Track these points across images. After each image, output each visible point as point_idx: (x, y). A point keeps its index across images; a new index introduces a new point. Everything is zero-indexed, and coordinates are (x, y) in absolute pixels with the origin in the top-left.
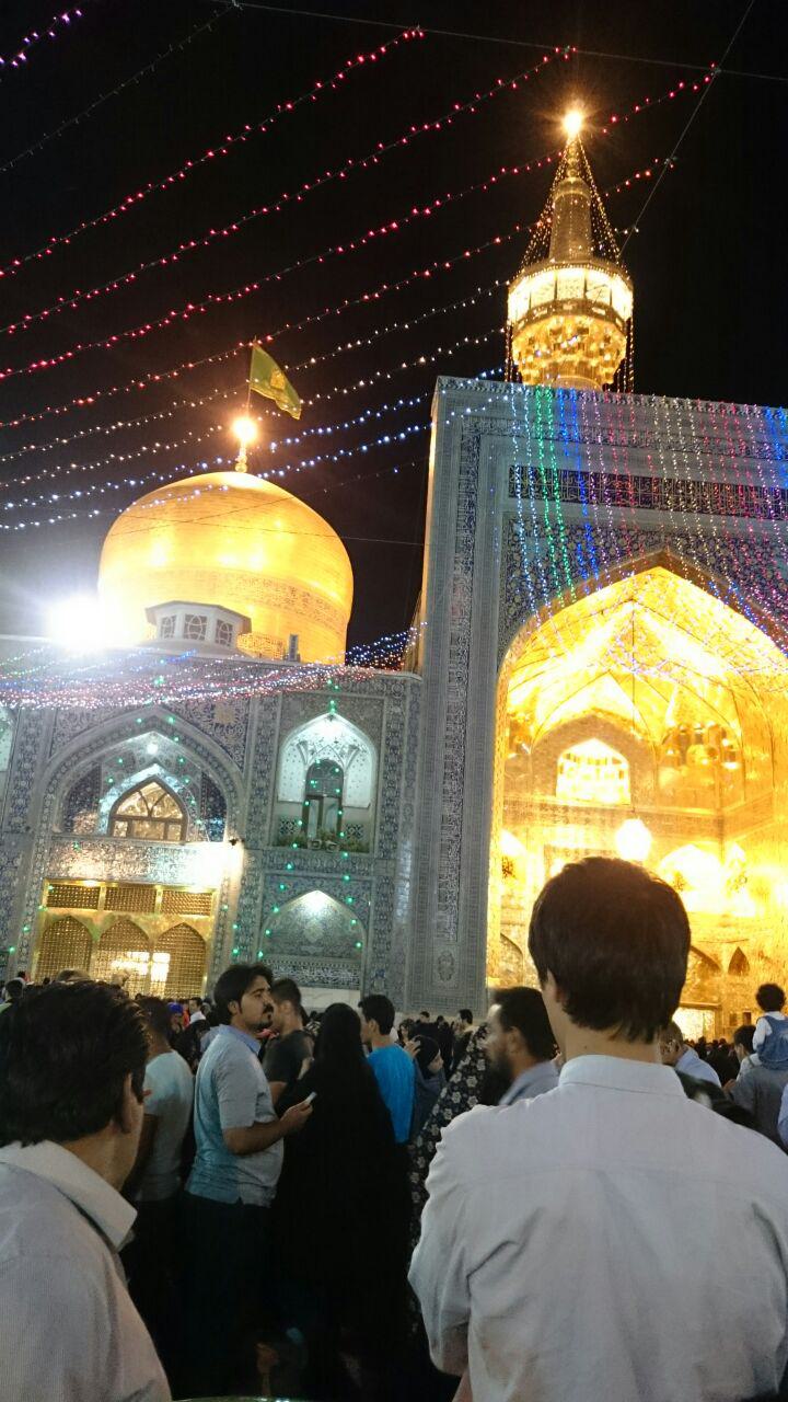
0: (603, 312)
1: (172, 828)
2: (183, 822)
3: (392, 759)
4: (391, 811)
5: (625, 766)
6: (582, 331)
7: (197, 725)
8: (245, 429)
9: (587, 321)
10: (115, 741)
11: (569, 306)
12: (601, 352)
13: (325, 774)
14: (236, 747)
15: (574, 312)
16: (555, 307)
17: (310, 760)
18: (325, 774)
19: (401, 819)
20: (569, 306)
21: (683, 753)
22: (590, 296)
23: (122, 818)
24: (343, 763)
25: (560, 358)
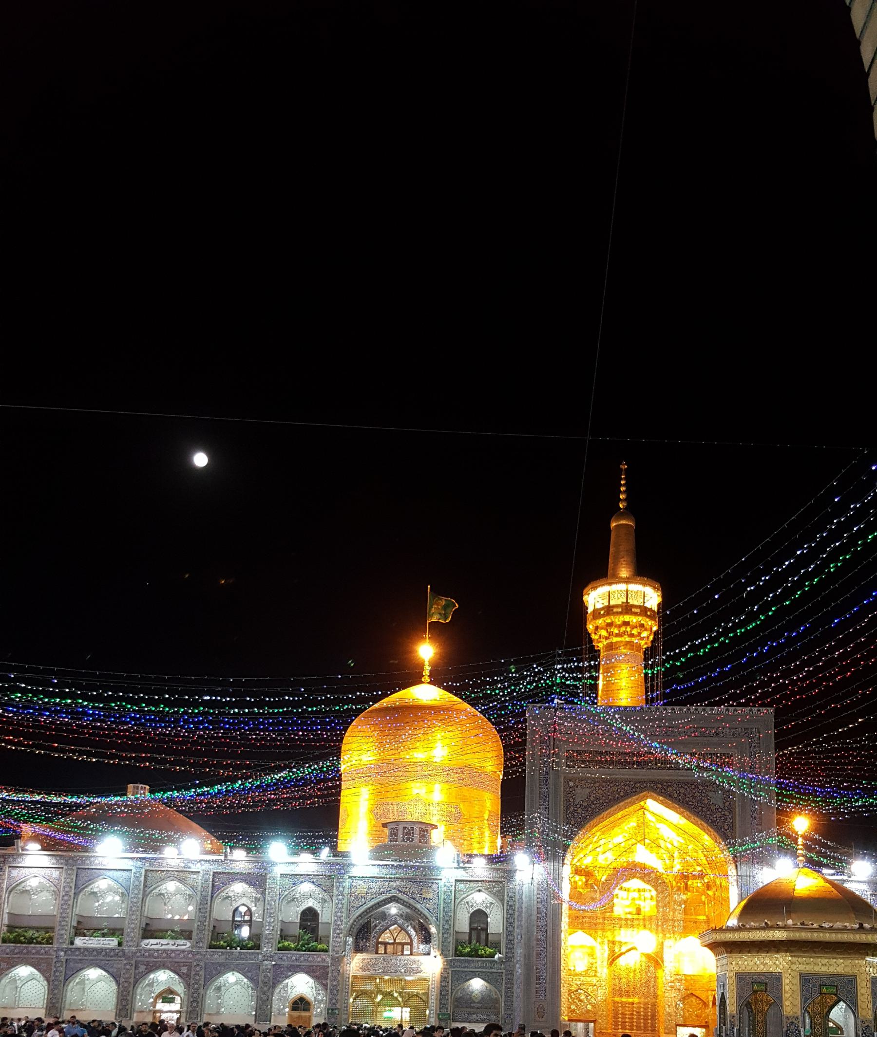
0: (638, 610)
1: (406, 947)
2: (411, 944)
3: (510, 912)
4: (511, 938)
5: (654, 893)
6: (626, 624)
7: (414, 899)
8: (426, 651)
9: (627, 618)
10: (377, 908)
11: (622, 603)
12: (639, 634)
13: (479, 916)
14: (434, 909)
15: (621, 613)
16: (609, 610)
17: (471, 911)
18: (479, 916)
19: (516, 941)
20: (622, 603)
21: (686, 884)
22: (631, 602)
23: (381, 943)
24: (487, 911)
25: (615, 640)
